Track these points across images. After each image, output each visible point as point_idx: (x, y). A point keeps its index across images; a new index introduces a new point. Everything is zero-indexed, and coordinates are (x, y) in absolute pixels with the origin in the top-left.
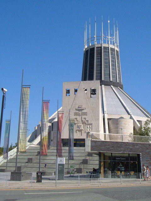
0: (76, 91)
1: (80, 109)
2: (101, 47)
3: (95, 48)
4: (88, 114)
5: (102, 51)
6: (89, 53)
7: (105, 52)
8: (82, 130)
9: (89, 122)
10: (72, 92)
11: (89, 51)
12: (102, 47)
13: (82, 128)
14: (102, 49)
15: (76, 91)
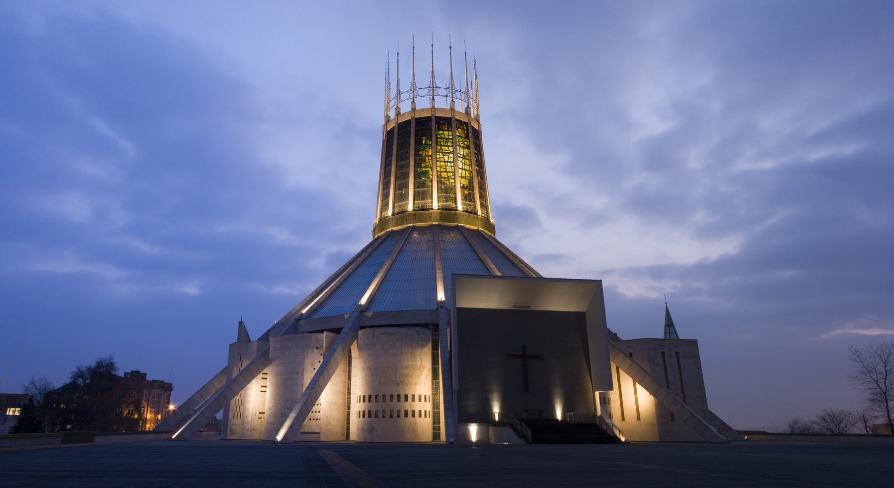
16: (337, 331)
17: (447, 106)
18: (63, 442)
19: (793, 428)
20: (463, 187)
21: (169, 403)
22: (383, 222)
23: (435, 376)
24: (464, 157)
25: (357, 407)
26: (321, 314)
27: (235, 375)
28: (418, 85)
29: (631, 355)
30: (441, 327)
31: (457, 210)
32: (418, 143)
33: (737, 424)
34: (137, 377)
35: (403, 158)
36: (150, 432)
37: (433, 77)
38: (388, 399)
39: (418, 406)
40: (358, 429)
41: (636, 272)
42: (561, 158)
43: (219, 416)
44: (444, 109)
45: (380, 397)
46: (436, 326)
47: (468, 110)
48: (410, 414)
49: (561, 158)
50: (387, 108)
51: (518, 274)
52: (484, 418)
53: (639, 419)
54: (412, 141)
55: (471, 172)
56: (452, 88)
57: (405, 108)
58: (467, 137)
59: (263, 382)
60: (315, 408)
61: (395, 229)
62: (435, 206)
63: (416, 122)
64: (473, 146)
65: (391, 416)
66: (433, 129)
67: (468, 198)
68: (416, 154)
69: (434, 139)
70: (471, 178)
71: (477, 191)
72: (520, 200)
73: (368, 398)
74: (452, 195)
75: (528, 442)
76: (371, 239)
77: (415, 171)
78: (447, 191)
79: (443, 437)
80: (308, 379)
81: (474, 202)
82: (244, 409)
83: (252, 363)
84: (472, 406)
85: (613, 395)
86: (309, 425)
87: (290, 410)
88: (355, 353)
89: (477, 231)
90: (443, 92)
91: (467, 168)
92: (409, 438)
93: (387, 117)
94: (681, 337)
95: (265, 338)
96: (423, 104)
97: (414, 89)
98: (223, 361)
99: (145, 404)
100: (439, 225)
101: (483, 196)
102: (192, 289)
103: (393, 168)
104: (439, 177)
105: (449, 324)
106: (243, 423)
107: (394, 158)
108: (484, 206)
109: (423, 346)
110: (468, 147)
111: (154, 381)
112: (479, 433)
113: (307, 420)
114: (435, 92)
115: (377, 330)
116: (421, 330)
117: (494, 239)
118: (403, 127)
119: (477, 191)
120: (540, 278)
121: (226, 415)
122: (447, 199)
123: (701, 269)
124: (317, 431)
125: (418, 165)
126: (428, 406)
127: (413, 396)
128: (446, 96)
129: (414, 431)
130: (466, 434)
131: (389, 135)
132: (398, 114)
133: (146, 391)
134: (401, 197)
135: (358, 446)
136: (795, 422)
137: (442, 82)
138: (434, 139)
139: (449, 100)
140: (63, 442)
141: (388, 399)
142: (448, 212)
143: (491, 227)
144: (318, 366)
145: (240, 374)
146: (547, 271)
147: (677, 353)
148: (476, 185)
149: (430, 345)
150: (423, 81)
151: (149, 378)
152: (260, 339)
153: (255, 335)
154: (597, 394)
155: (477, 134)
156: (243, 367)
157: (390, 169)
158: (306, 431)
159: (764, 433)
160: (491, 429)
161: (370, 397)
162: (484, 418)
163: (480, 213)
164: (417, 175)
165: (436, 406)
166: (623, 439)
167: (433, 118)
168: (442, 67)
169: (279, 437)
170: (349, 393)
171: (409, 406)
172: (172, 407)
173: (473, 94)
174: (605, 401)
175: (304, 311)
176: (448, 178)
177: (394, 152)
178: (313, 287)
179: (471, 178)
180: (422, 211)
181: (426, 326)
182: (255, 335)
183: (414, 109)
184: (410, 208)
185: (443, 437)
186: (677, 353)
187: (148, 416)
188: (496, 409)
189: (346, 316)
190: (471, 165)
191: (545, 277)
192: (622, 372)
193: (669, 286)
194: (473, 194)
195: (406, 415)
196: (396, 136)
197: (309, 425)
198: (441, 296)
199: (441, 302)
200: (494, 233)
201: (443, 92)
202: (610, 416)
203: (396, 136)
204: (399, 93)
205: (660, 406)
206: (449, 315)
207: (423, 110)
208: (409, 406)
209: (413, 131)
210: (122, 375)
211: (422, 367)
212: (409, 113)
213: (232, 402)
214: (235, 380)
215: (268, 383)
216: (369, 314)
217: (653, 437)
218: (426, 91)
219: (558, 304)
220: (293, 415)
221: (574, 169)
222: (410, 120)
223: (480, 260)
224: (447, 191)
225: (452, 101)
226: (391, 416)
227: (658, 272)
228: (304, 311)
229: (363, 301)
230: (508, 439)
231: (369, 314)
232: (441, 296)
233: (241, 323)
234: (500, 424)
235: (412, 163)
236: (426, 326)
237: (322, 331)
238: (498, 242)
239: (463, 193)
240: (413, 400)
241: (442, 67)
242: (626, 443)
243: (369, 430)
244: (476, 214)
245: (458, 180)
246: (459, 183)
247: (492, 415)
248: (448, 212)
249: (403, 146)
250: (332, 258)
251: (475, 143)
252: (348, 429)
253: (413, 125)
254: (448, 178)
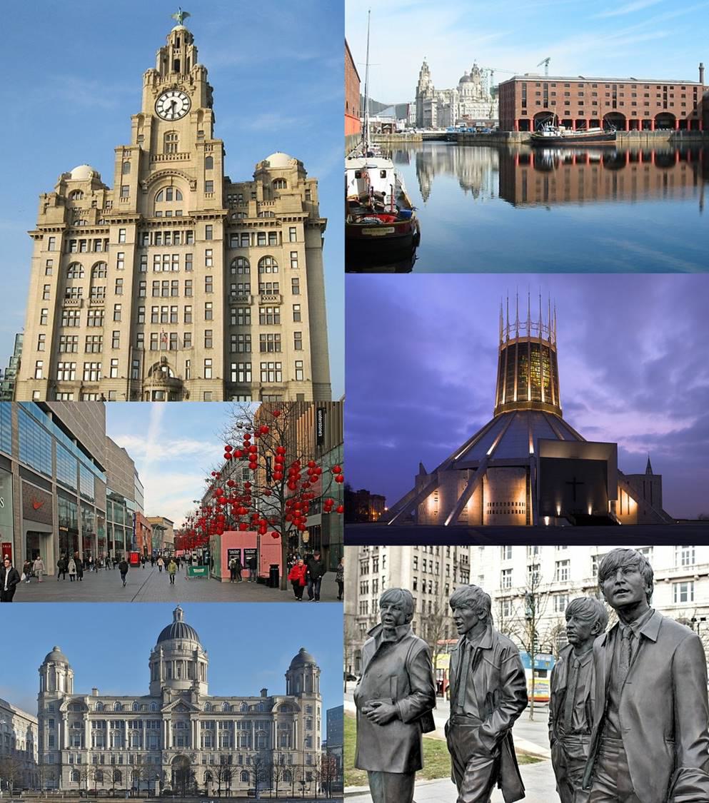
12: (529, 344)
16: (475, 469)
17: (537, 336)
19: (700, 518)
20: (545, 388)
21: (384, 507)
22: (500, 407)
23: (528, 493)
24: (546, 370)
25: (486, 508)
26: (467, 459)
27: (420, 492)
29: (628, 483)
30: (531, 467)
31: (541, 401)
32: (520, 359)
33: (674, 516)
34: (364, 493)
35: (511, 368)
36: (375, 522)
37: (529, 316)
38: (503, 505)
39: (518, 508)
40: (488, 520)
41: (635, 439)
42: (600, 373)
43: (413, 513)
44: (535, 338)
45: (499, 504)
46: (529, 467)
47: (549, 338)
48: (515, 512)
49: (600, 373)
50: (501, 336)
51: (574, 439)
52: (552, 513)
53: (629, 513)
54: (516, 358)
55: (550, 379)
56: (541, 325)
57: (512, 336)
58: (549, 357)
59: (436, 496)
60: (464, 509)
61: (506, 412)
62: (529, 399)
63: (519, 346)
64: (551, 363)
65: (505, 513)
66: (529, 350)
67: (548, 395)
68: (518, 367)
69: (529, 357)
70: (550, 382)
71: (553, 390)
72: (578, 400)
73: (492, 504)
74: (539, 393)
75: (573, 524)
76: (493, 417)
77: (518, 377)
78: (536, 390)
79: (532, 523)
80: (460, 495)
81: (552, 397)
82: (426, 509)
83: (428, 486)
84: (546, 508)
85: (618, 503)
86: (461, 517)
87: (452, 510)
88: (485, 481)
89: (552, 414)
91: (548, 376)
92: (514, 524)
93: (501, 341)
94: (654, 474)
95: (435, 472)
96: (523, 334)
97: (517, 324)
98: (412, 484)
99: (370, 507)
100: (531, 410)
101: (556, 394)
102: (390, 445)
103: (505, 382)
104: (532, 381)
105: (536, 465)
106: (426, 517)
107: (506, 368)
108: (557, 400)
109: (522, 477)
110: (549, 363)
111: (374, 495)
112: (550, 521)
113: (460, 516)
115: (497, 469)
116: (522, 469)
117: (561, 419)
118: (511, 348)
119: (553, 390)
120: (585, 441)
121: (417, 513)
122: (536, 395)
123: (672, 437)
124: (466, 520)
125: (519, 373)
126: (524, 508)
127: (516, 503)
129: (517, 520)
130: (544, 521)
131: (503, 353)
132: (508, 339)
133: (370, 501)
134: (510, 393)
135: (487, 528)
136: (702, 515)
137: (535, 320)
138: (529, 357)
141: (503, 505)
142: (537, 402)
143: (560, 412)
144: (465, 488)
145: (423, 492)
146: (589, 437)
147: (651, 482)
148: (553, 387)
149: (525, 478)
150: (523, 319)
151: (371, 494)
152: (432, 473)
153: (429, 471)
154: (610, 502)
155: (554, 355)
156: (425, 487)
157: (503, 375)
158: (460, 520)
159: (687, 520)
160: (556, 519)
161: (494, 504)
162: (552, 513)
163: (554, 404)
164: (519, 380)
165: (528, 508)
166: (620, 523)
167: (529, 344)
168: (535, 309)
169: (446, 524)
170: (483, 502)
171: (514, 508)
172: (386, 509)
173: (553, 329)
174: (613, 505)
175: (456, 458)
176: (537, 382)
177: (506, 365)
178: (461, 445)
179: (550, 382)
180: (522, 401)
181: (523, 467)
182: (429, 471)
183: (517, 337)
184: (515, 399)
185: (532, 523)
186: (651, 482)
187: (374, 514)
188: (559, 510)
189: (480, 461)
190: (550, 374)
191: (588, 440)
192: (623, 491)
193: (651, 447)
194: (551, 392)
195: (513, 513)
196: (506, 355)
197: (461, 517)
198: (532, 451)
199: (532, 454)
200: (561, 415)
202: (615, 512)
203: (506, 355)
204: (508, 326)
205: (639, 508)
206: (536, 461)
208: (514, 508)
209: (517, 351)
210: (356, 492)
211: (521, 488)
212: (514, 339)
213: (420, 506)
214: (420, 494)
215: (438, 496)
216: (493, 460)
217: (635, 522)
218: (525, 325)
219: (593, 456)
220: (453, 513)
221: (607, 380)
222: (515, 344)
223: (554, 431)
224: (536, 390)
225: (541, 333)
226: (505, 513)
227: (646, 439)
228: (456, 458)
229: (489, 453)
230: (564, 523)
231: (493, 460)
232: (532, 451)
233: (421, 464)
234: (561, 516)
235: (516, 372)
236: (523, 467)
237: (466, 469)
238: (563, 421)
239: (545, 391)
240: (516, 505)
241: (535, 309)
242: (621, 525)
243: (493, 520)
244: (552, 404)
245: (543, 384)
246: (543, 385)
247: (557, 512)
248: (537, 402)
249: (511, 360)
250: (471, 428)
251: (553, 361)
252: (482, 519)
254: (537, 382)
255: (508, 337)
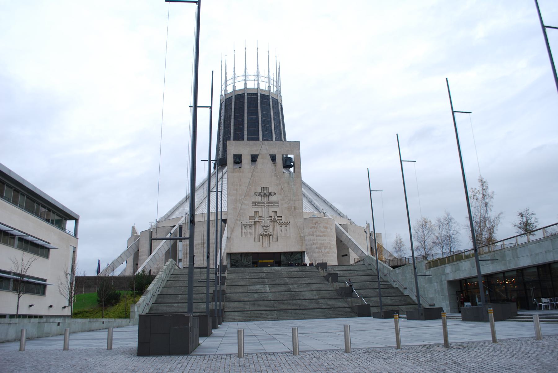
0: (254, 159)
1: (265, 193)
2: (256, 94)
3: (246, 95)
4: (279, 204)
5: (259, 101)
6: (233, 103)
7: (262, 103)
8: (269, 235)
9: (283, 221)
10: (246, 160)
11: (233, 100)
12: (259, 95)
13: (271, 230)
14: (259, 98)
15: (254, 159)
18: (328, 229)
28: (249, 72)
90: (253, 78)
114: (259, 79)
128: (255, 80)
139: (256, 82)
140: (328, 229)
183: (246, 87)
201: (263, 79)
207: (252, 89)
253: (246, 98)
255: (234, 86)
